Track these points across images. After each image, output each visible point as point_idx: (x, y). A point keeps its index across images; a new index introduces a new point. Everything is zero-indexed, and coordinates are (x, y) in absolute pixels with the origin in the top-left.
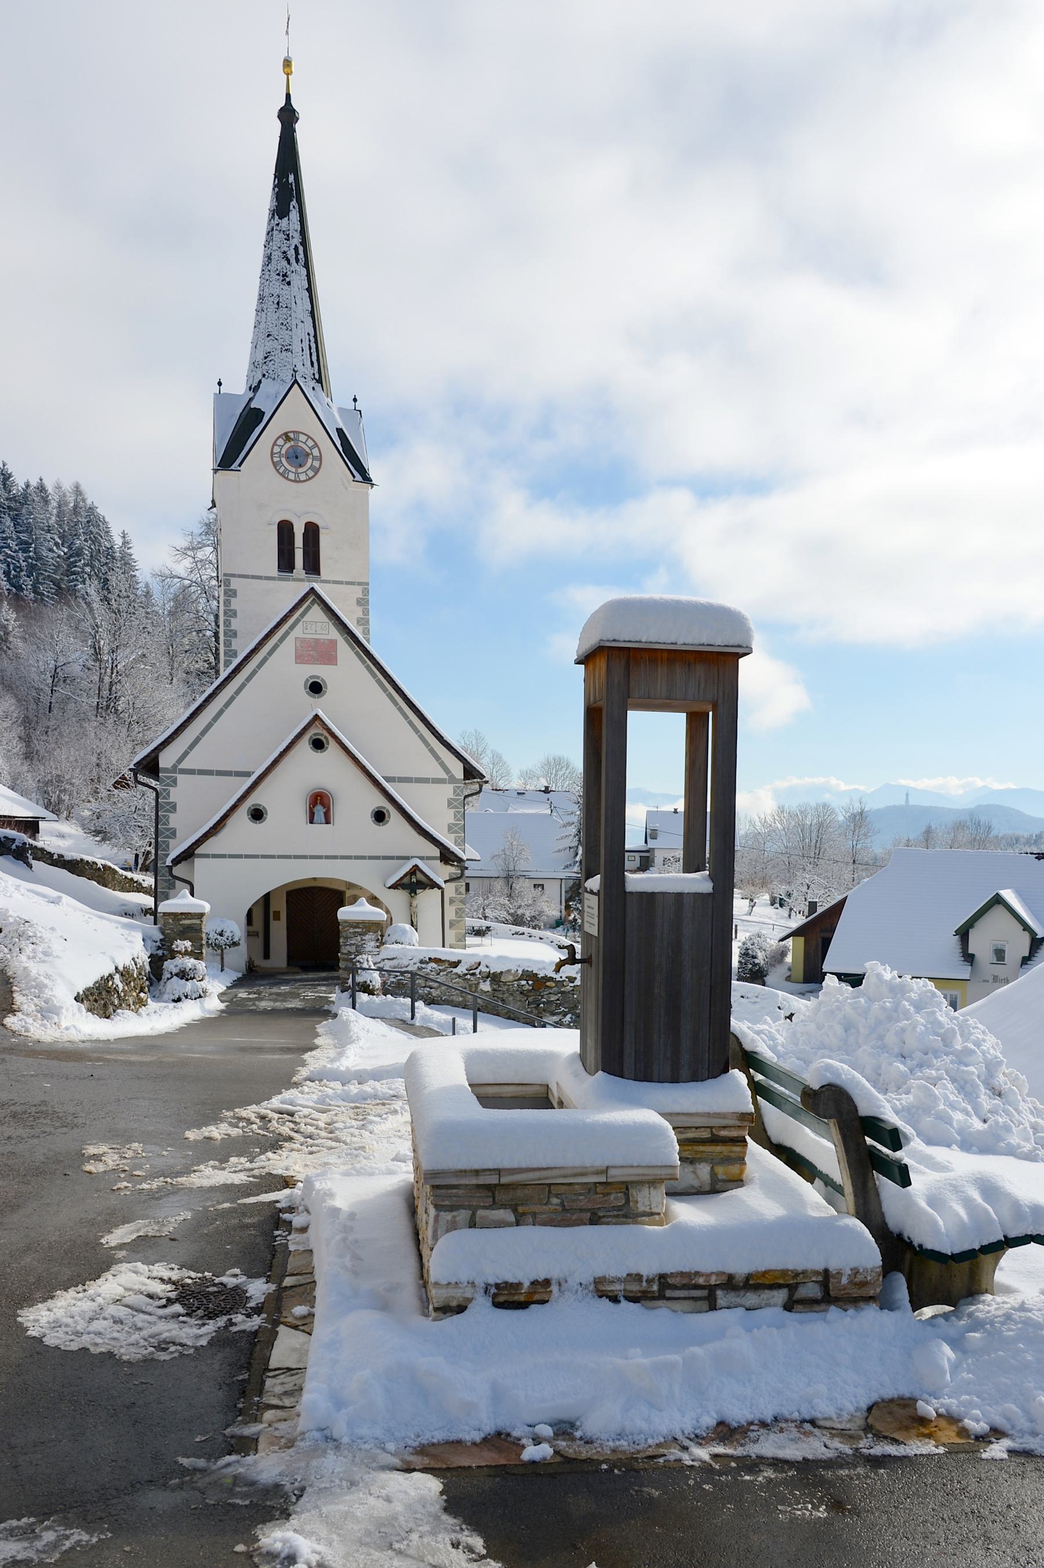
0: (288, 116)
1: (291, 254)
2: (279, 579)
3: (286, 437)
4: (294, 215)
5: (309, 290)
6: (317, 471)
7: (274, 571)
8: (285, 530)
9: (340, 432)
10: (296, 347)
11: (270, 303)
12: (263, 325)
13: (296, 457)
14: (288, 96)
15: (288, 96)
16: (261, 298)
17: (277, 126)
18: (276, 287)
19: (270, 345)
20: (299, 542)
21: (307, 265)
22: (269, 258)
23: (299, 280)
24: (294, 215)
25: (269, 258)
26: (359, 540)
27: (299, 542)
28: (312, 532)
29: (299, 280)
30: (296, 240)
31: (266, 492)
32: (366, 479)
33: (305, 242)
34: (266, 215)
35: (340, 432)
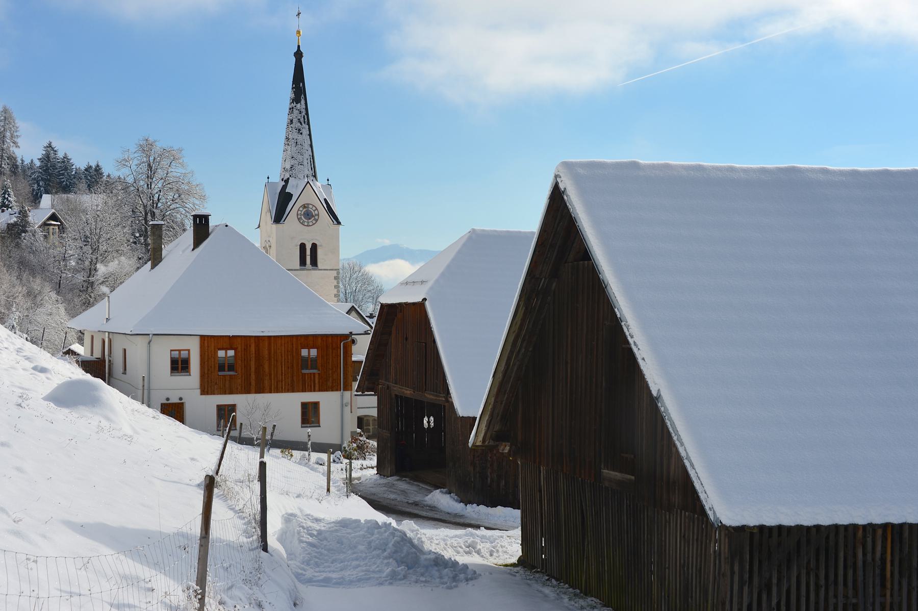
0: (299, 55)
1: (302, 120)
2: (301, 270)
3: (304, 206)
4: (303, 102)
5: (310, 135)
6: (317, 220)
7: (298, 267)
8: (303, 247)
9: (325, 200)
10: (305, 163)
11: (292, 142)
12: (289, 152)
13: (308, 215)
14: (299, 46)
15: (299, 46)
16: (287, 139)
17: (293, 60)
18: (295, 135)
19: (293, 162)
20: (308, 252)
21: (309, 124)
22: (292, 121)
23: (305, 132)
24: (303, 102)
25: (292, 121)
26: (335, 250)
27: (308, 252)
28: (314, 247)
29: (305, 132)
30: (304, 114)
31: (294, 230)
32: (339, 223)
33: (307, 114)
34: (288, 101)
35: (325, 200)
